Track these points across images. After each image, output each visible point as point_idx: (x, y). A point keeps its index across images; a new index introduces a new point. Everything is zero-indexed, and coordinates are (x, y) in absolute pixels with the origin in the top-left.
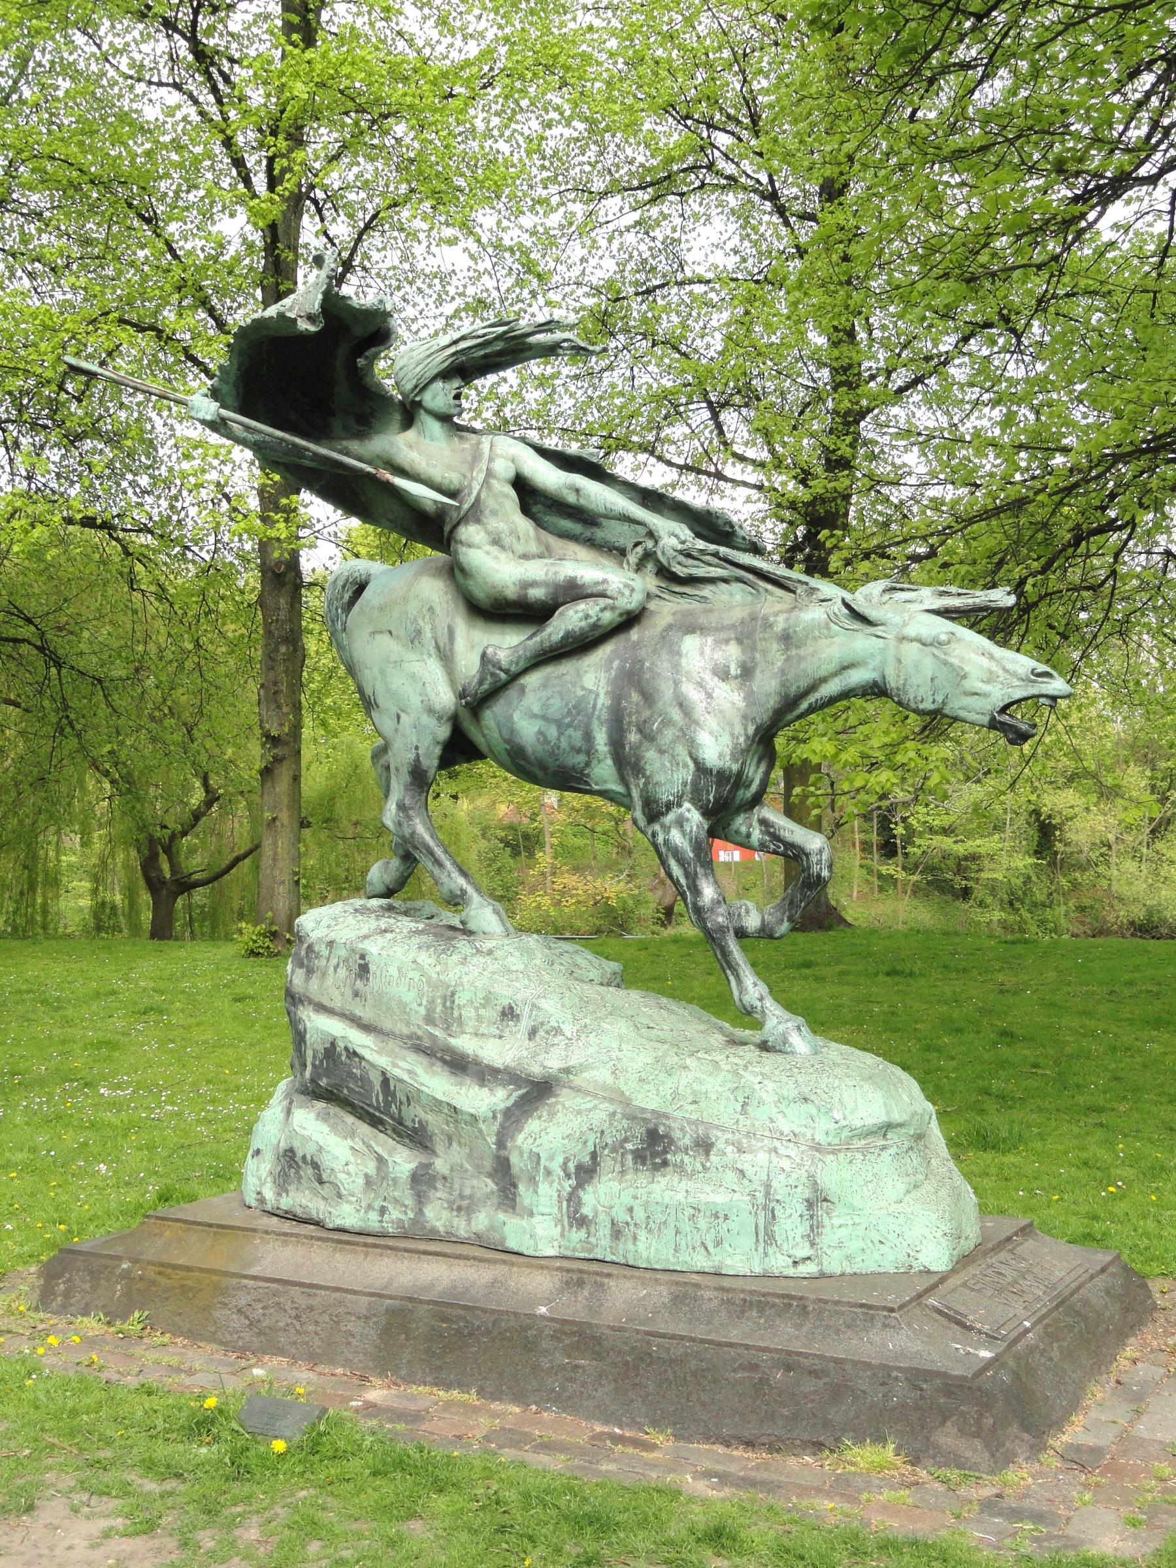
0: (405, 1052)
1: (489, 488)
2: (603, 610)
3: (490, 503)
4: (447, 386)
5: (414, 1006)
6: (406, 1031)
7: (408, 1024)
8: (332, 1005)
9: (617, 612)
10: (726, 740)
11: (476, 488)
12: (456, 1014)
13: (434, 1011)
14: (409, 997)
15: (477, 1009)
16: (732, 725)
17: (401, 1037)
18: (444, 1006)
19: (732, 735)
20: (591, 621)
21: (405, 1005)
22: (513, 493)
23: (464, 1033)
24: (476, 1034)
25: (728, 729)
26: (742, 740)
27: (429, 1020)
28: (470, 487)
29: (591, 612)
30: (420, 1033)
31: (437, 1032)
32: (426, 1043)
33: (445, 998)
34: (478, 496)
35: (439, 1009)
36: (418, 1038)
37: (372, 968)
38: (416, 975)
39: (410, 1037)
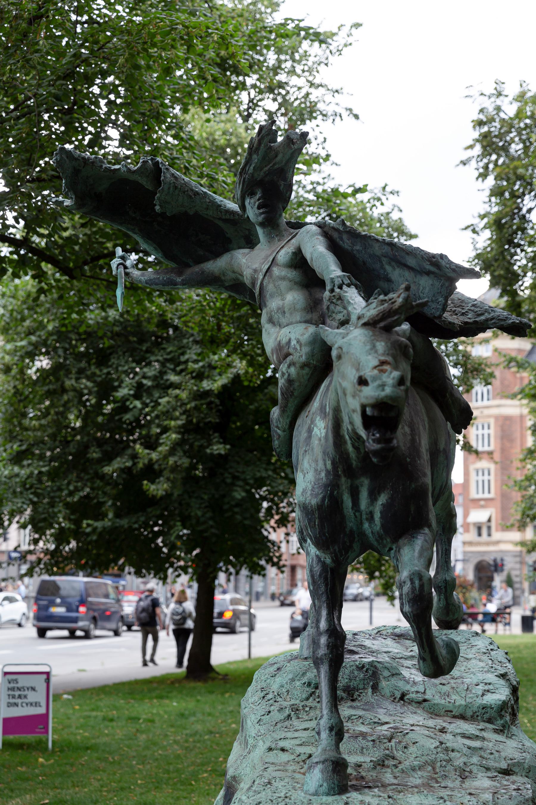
1: (271, 276)
2: (289, 366)
3: (270, 287)
4: (252, 201)
9: (297, 365)
10: (310, 476)
11: (261, 277)
16: (316, 461)
19: (316, 470)
20: (286, 376)
22: (292, 274)
25: (313, 465)
26: (323, 474)
28: (258, 279)
29: (284, 370)
34: (262, 284)
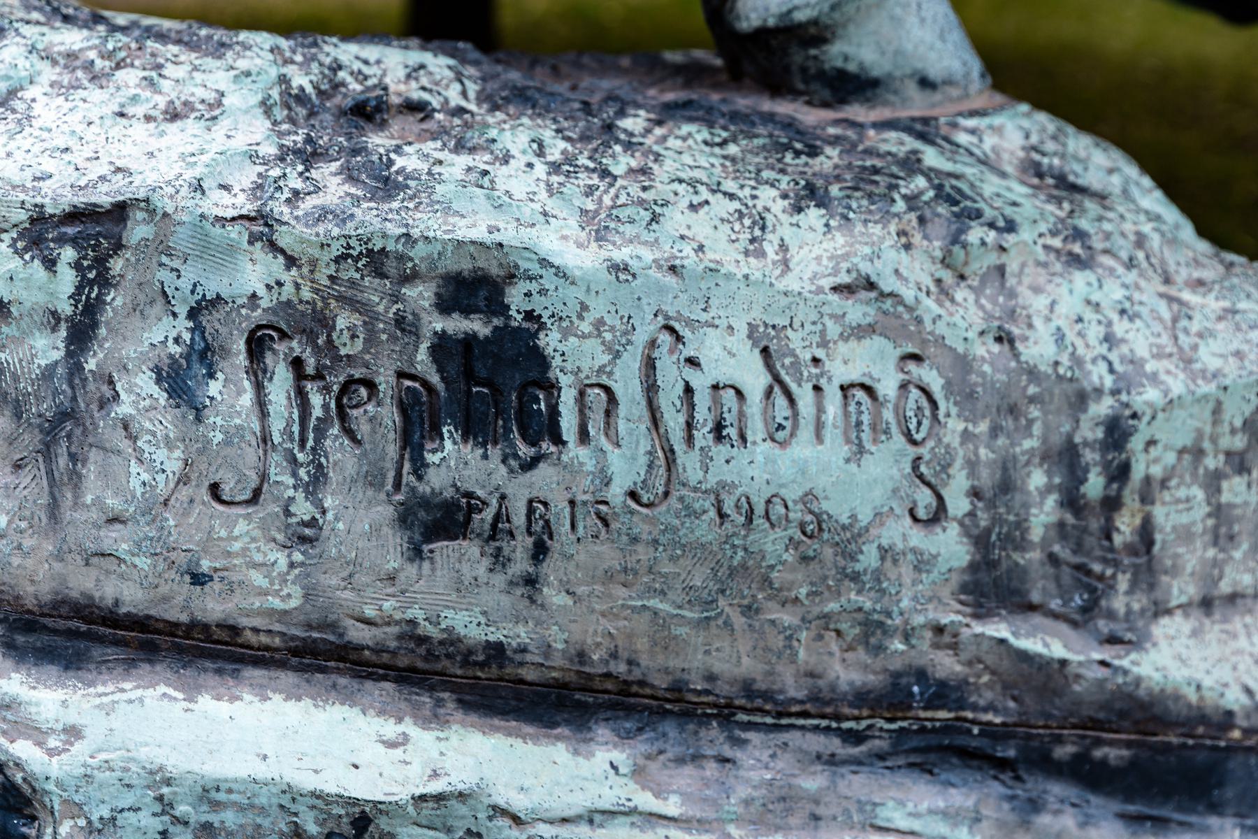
0: (858, 784)
5: (900, 532)
6: (847, 671)
7: (872, 630)
8: (213, 606)
12: (1126, 526)
13: (1016, 537)
14: (857, 481)
15: (1213, 482)
17: (821, 708)
18: (1072, 501)
21: (849, 539)
23: (1160, 610)
24: (1207, 604)
27: (992, 584)
30: (947, 665)
31: (1047, 642)
32: (992, 708)
33: (1067, 458)
35: (1043, 514)
36: (944, 693)
37: (572, 355)
38: (871, 361)
39: (891, 698)
